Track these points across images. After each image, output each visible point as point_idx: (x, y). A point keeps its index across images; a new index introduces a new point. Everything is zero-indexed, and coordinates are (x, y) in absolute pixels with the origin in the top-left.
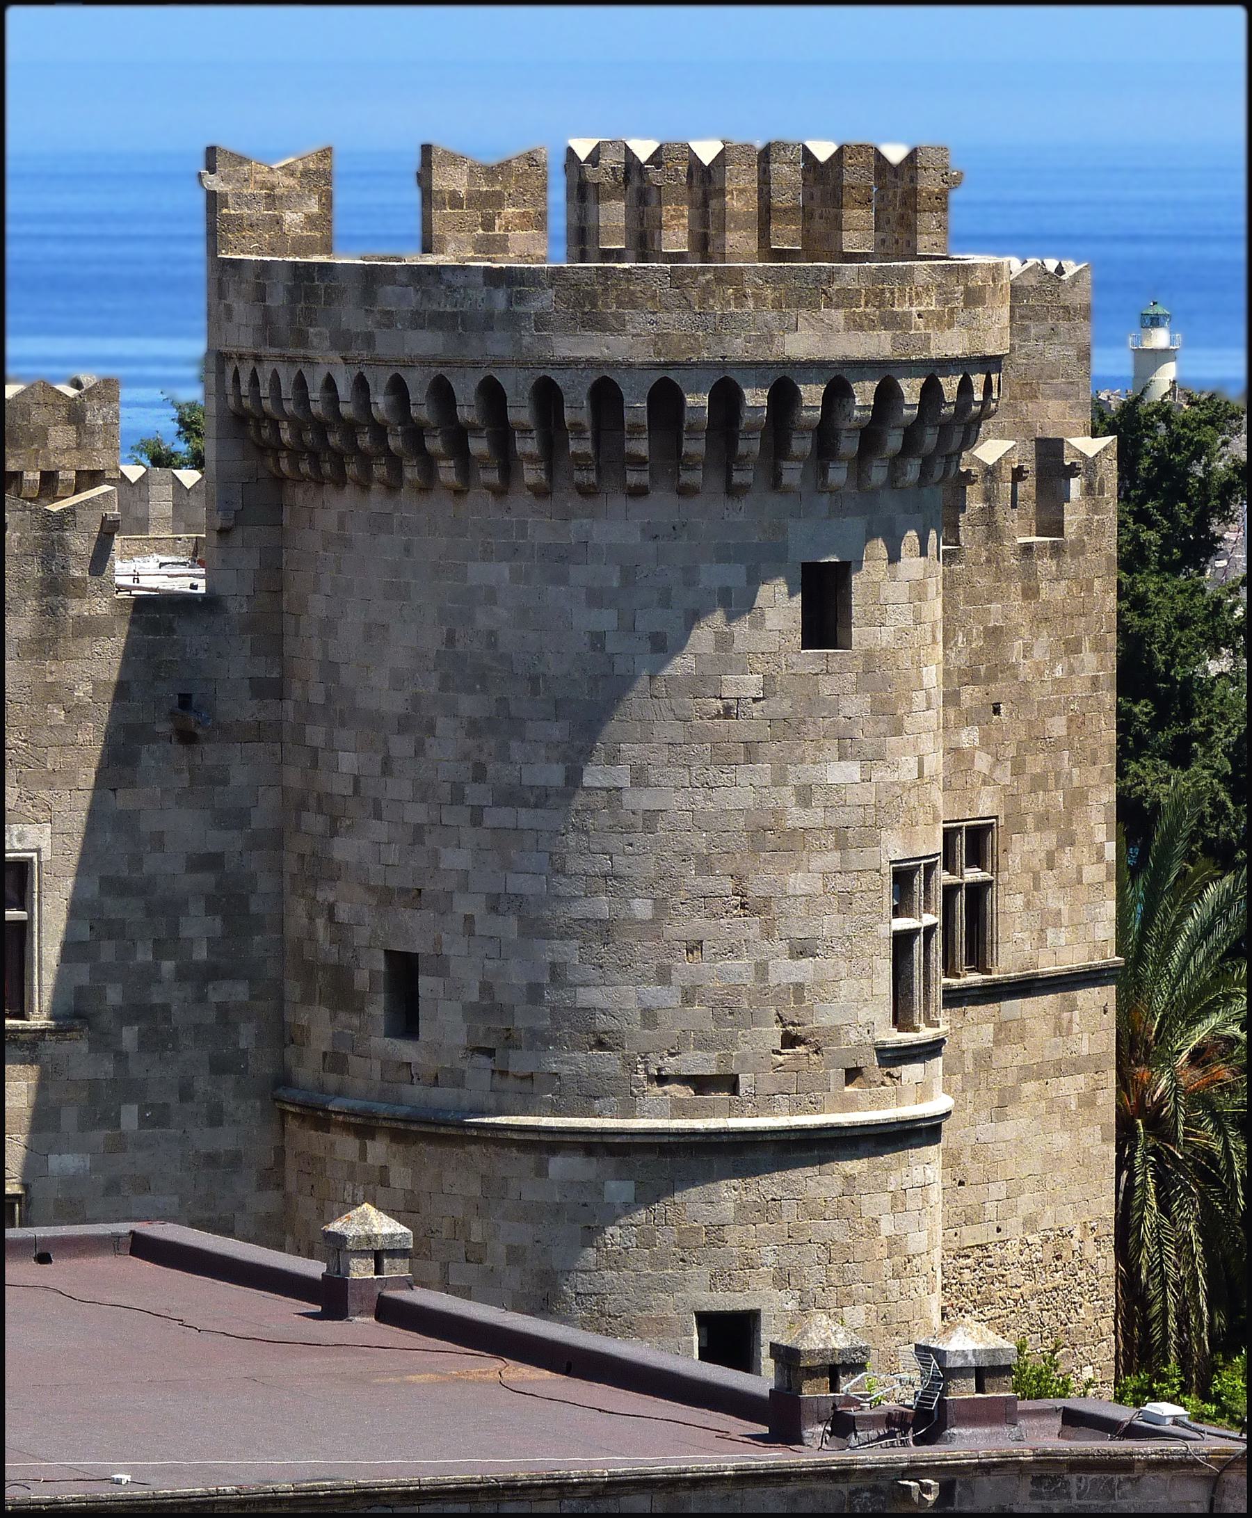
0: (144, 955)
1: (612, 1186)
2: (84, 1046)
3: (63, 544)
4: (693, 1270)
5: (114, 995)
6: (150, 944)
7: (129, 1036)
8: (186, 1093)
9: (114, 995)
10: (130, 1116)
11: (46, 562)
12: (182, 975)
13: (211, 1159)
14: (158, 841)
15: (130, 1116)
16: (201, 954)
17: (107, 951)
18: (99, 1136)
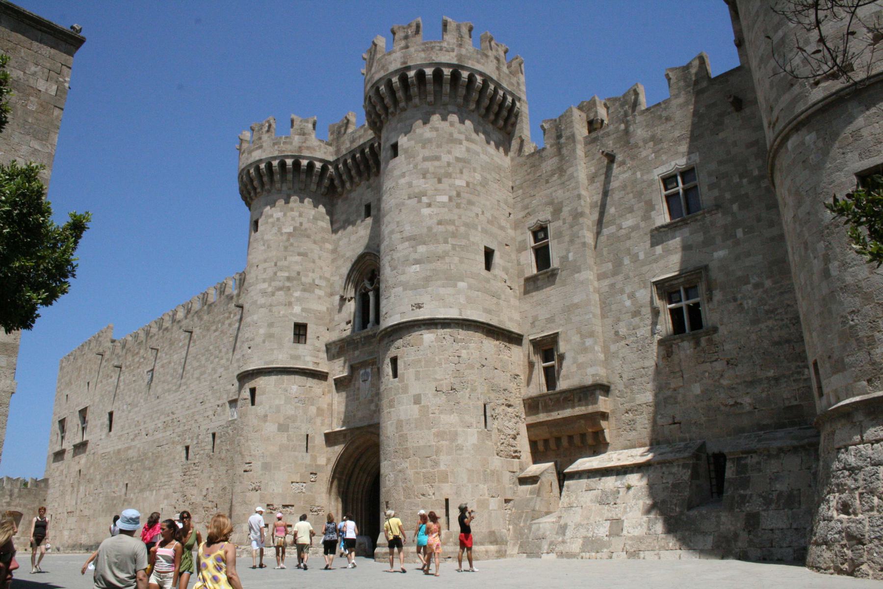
0: (736, 180)
1: (807, 138)
2: (720, 215)
3: (689, 73)
4: (850, 155)
5: (728, 196)
6: (737, 176)
7: (735, 207)
8: (759, 220)
9: (728, 196)
10: (740, 233)
11: (685, 81)
12: (750, 183)
13: (772, 239)
14: (735, 144)
15: (740, 233)
16: (756, 173)
17: (723, 183)
18: (729, 243)
